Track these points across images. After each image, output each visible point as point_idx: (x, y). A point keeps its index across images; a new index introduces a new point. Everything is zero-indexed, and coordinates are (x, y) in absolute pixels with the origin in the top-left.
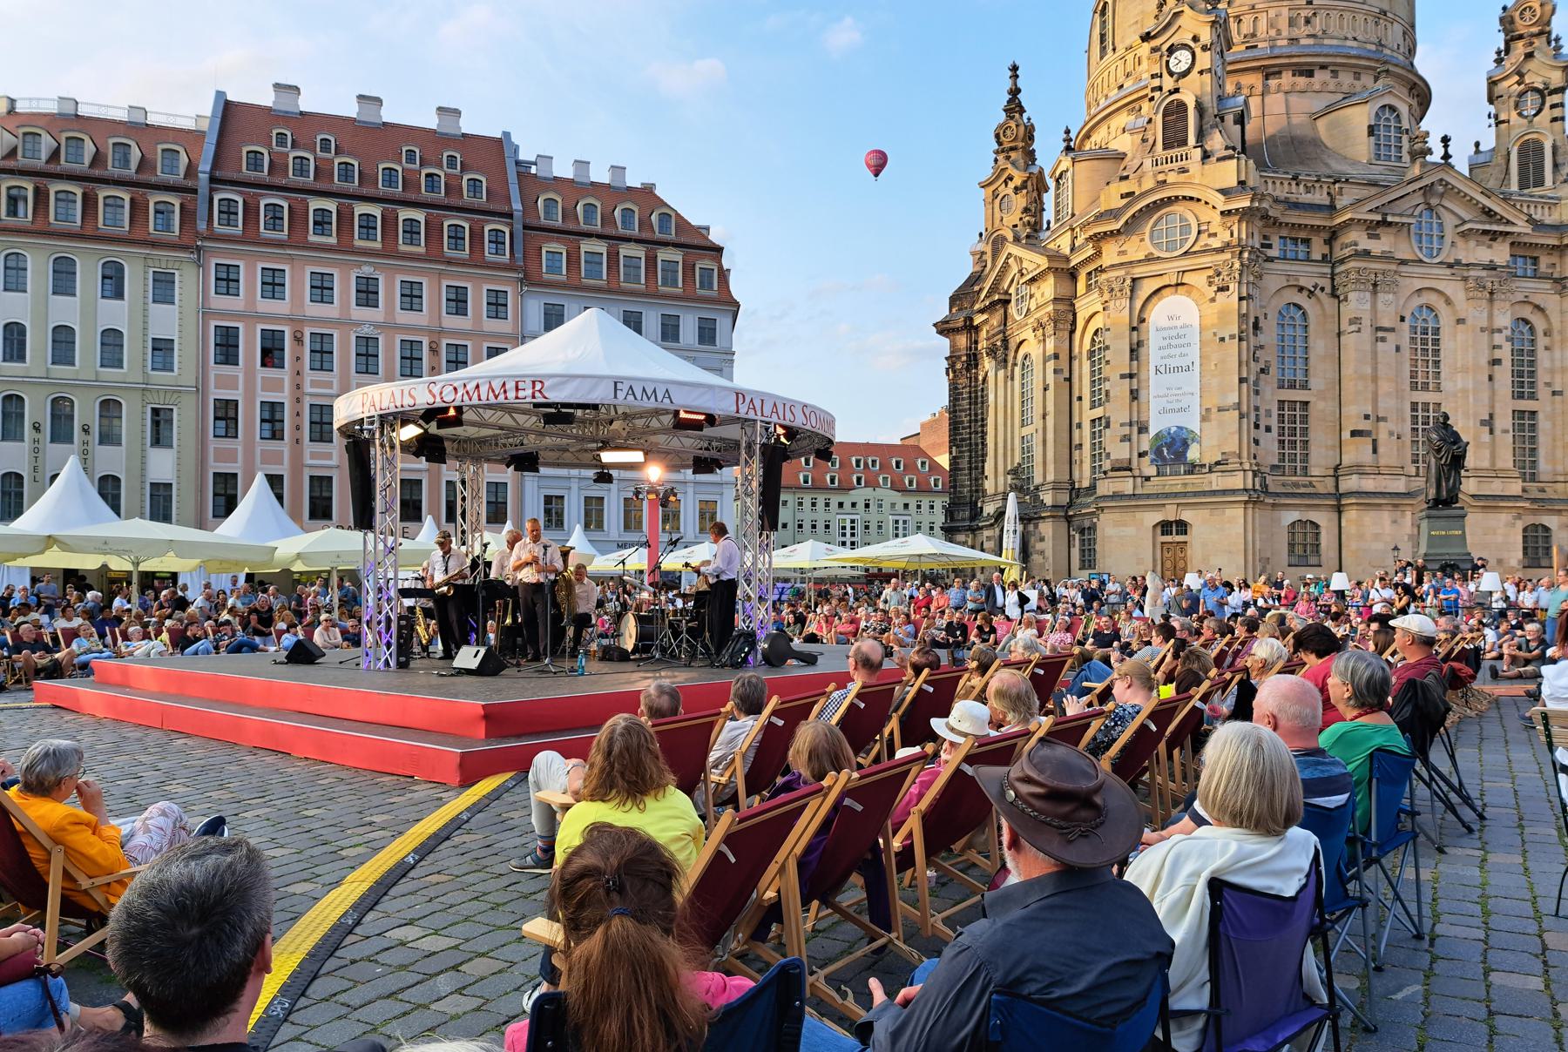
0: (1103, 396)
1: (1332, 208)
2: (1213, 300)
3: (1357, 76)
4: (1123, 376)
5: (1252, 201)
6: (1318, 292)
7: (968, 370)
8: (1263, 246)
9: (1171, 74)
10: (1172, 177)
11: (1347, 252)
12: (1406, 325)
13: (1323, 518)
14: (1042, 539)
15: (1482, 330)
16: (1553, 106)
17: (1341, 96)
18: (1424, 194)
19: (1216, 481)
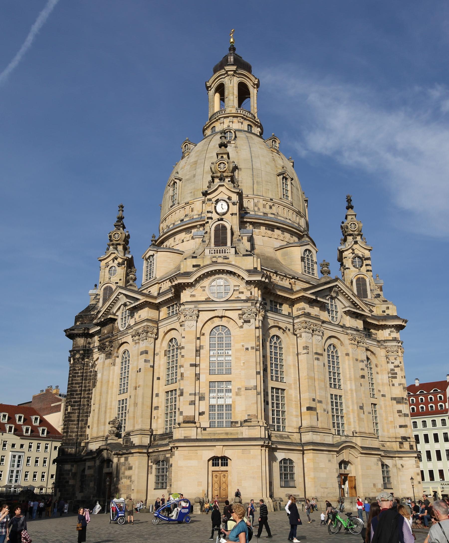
0: (179, 377)
2: (241, 327)
4: (192, 365)
5: (262, 278)
6: (287, 331)
7: (83, 359)
11: (300, 312)
12: (326, 354)
13: (295, 457)
14: (130, 468)
16: (367, 265)
17: (286, 243)
19: (246, 432)
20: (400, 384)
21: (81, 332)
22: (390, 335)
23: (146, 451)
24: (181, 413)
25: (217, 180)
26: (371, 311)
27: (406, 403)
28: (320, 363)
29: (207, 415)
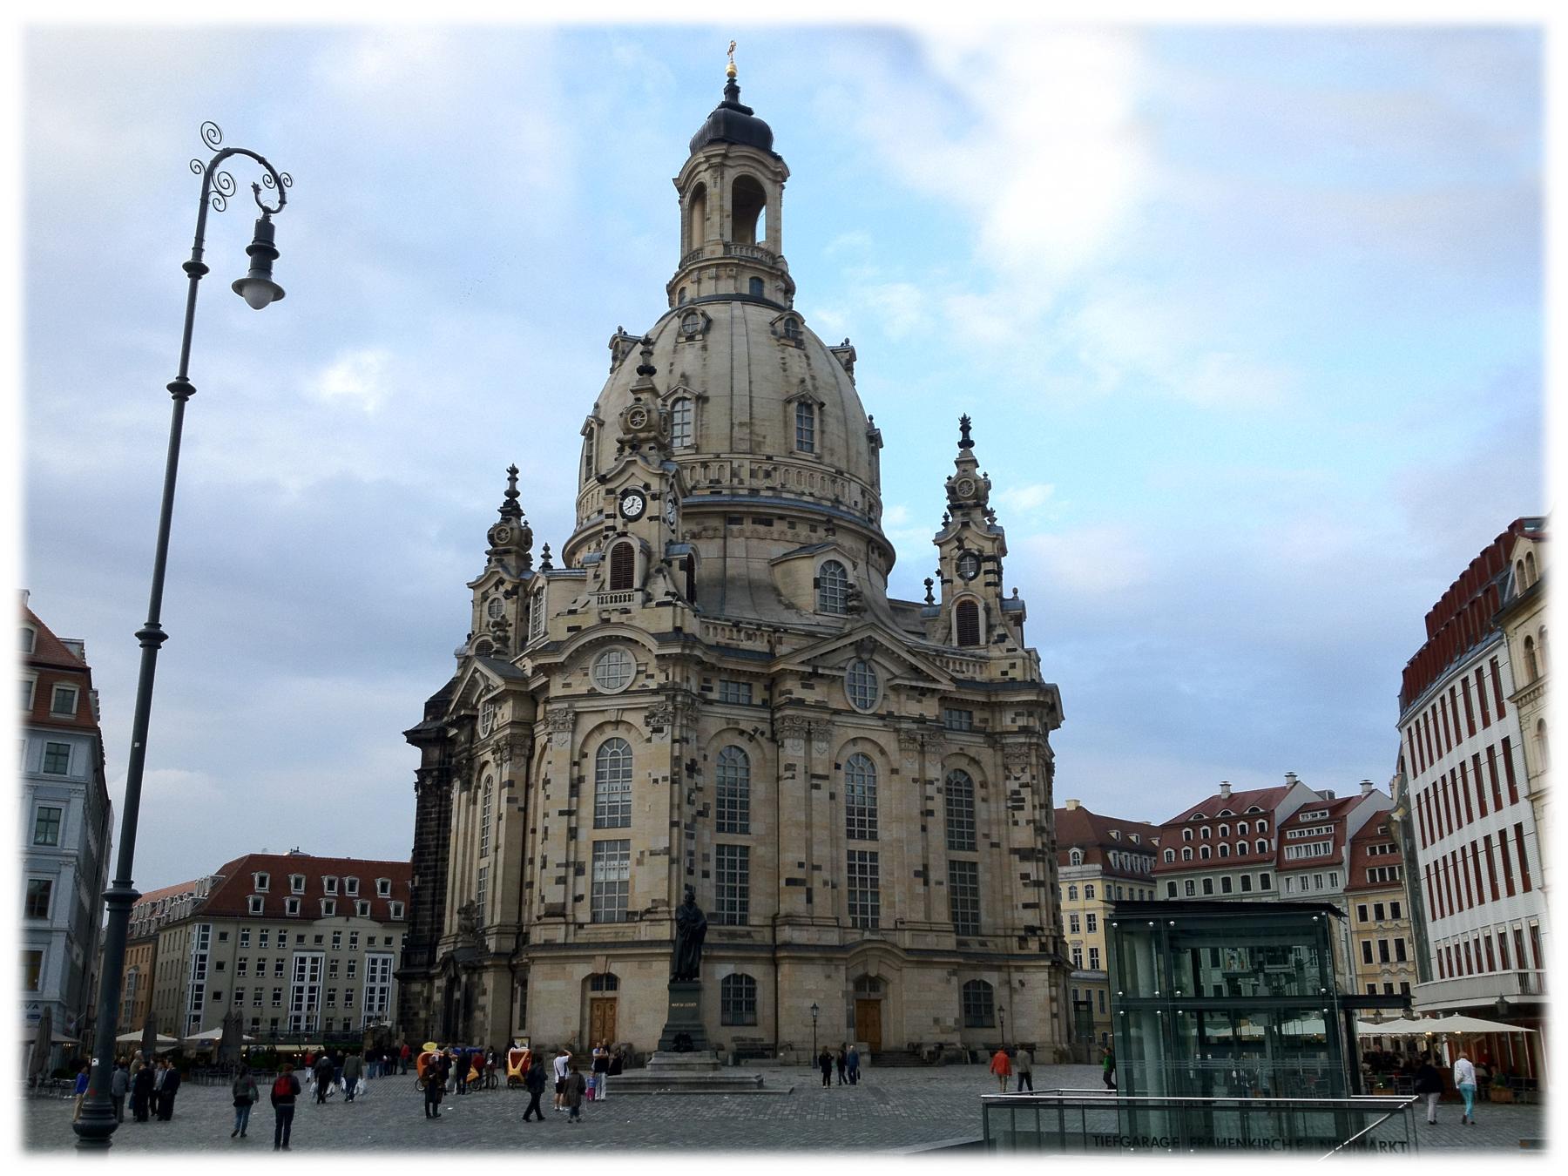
1: (771, 656)
2: (649, 740)
3: (813, 529)
4: (561, 813)
5: (684, 647)
6: (758, 736)
7: (439, 786)
8: (703, 688)
9: (624, 515)
10: (615, 618)
11: (783, 699)
15: (915, 781)
16: (987, 572)
17: (798, 546)
18: (857, 649)
19: (645, 932)
20: (1028, 822)
21: (433, 735)
22: (1014, 721)
23: (505, 962)
24: (543, 898)
25: (628, 451)
26: (953, 679)
27: (1038, 860)
28: (821, 795)
29: (587, 901)
